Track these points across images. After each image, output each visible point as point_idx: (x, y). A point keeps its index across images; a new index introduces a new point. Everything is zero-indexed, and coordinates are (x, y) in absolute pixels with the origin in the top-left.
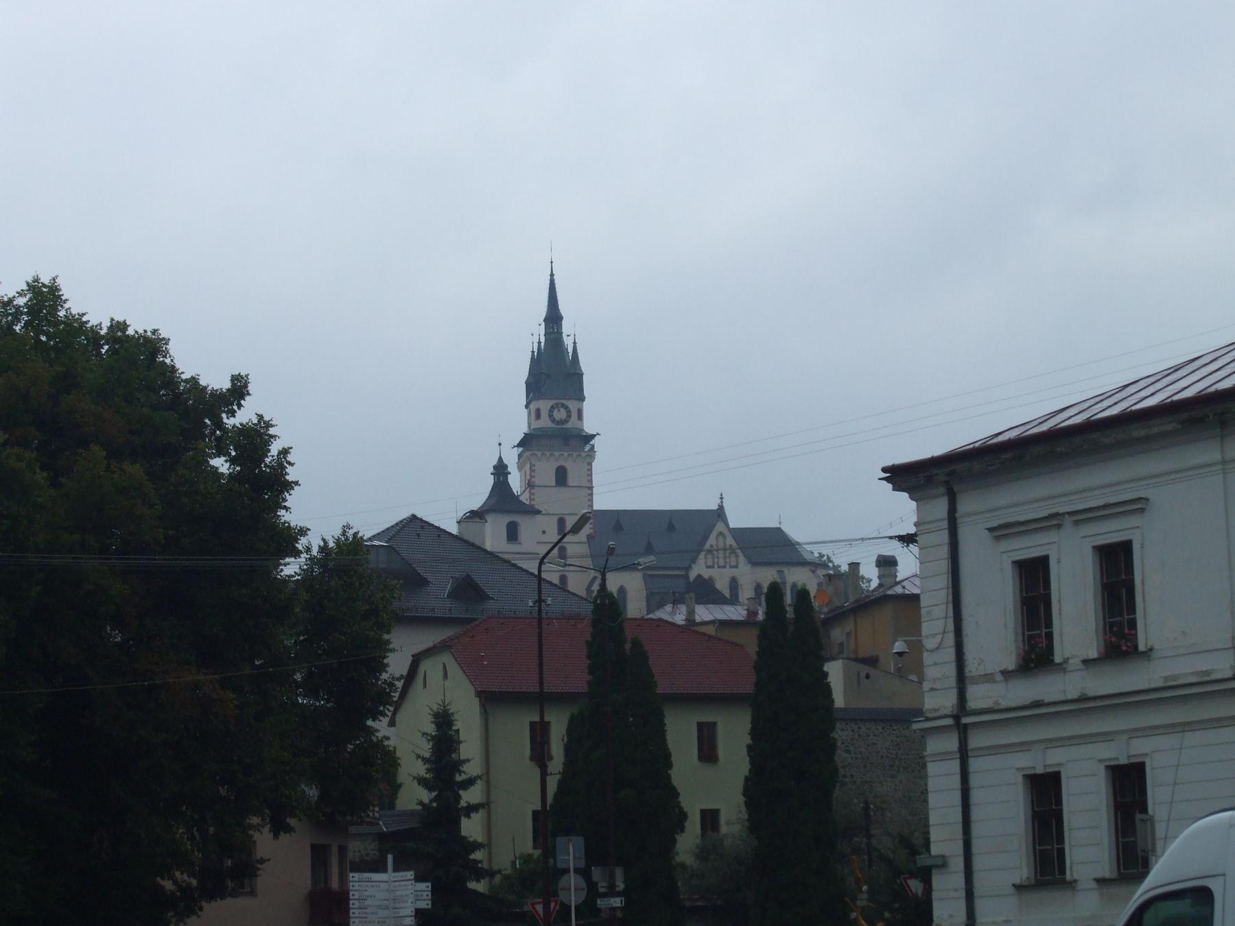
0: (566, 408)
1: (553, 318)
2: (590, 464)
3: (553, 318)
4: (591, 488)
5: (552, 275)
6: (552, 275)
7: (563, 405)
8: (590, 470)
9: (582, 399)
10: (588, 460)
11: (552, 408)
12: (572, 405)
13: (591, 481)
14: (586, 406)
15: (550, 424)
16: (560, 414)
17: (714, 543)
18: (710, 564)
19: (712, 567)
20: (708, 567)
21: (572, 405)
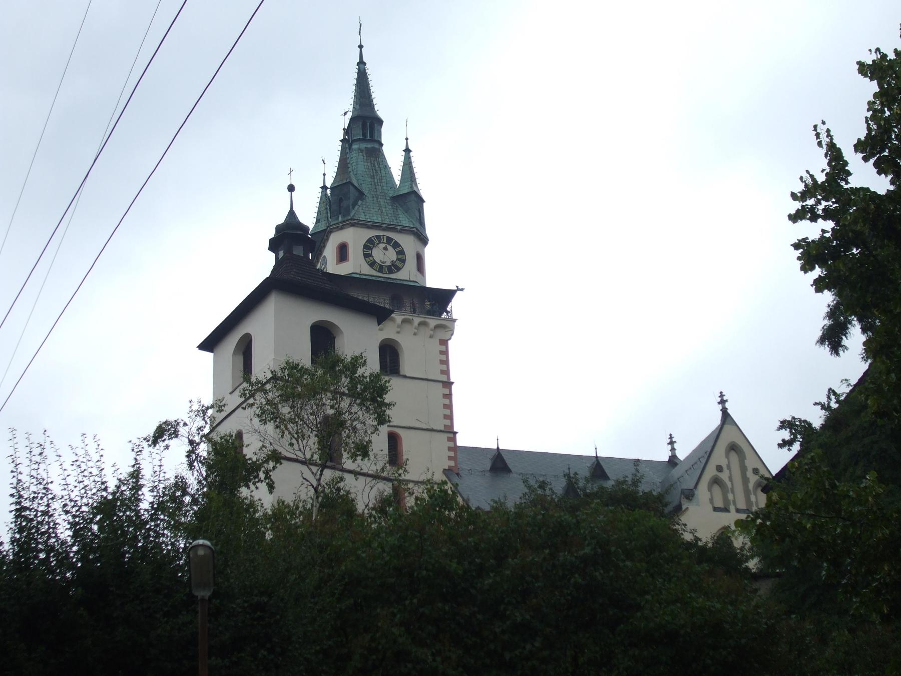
0: (396, 245)
1: (364, 127)
2: (444, 342)
3: (364, 127)
4: (448, 384)
5: (361, 63)
6: (361, 63)
7: (389, 240)
8: (446, 353)
9: (424, 241)
10: (441, 335)
11: (369, 246)
12: (407, 242)
13: (446, 372)
14: (429, 253)
15: (366, 270)
16: (384, 255)
17: (723, 462)
18: (719, 504)
19: (726, 510)
20: (715, 509)
21: (407, 242)
